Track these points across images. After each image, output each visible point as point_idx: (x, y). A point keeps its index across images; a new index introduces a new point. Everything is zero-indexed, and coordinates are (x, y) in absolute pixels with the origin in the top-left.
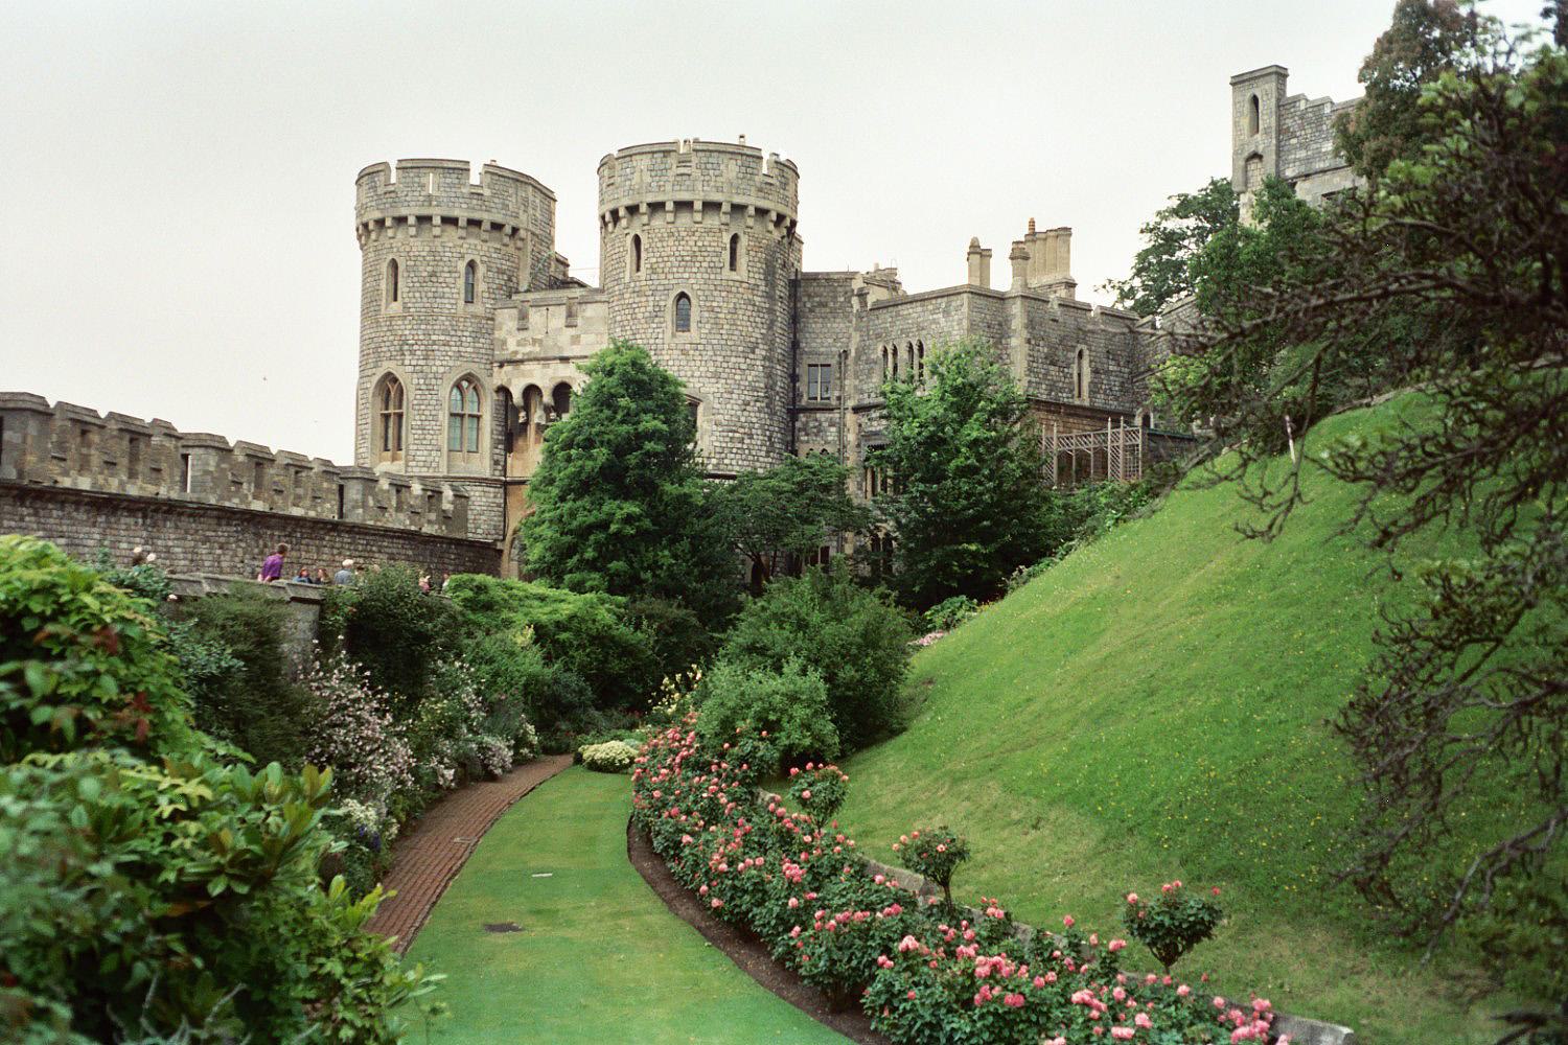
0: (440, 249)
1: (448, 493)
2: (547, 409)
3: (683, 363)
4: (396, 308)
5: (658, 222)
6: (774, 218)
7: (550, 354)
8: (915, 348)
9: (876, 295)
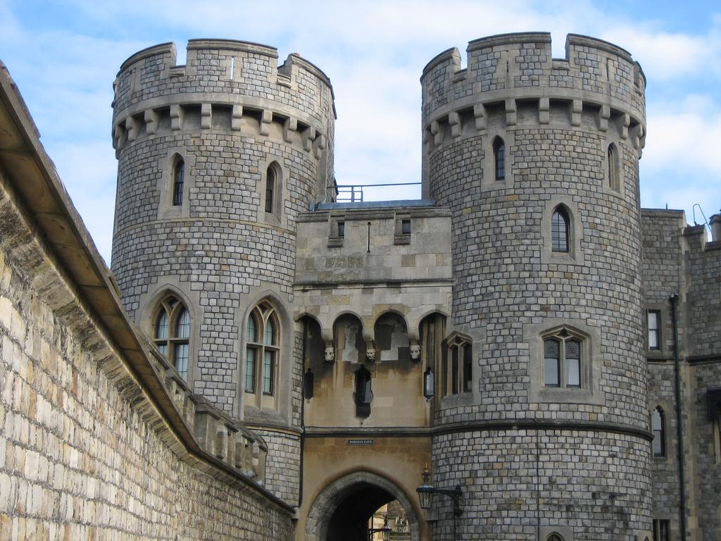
0: (240, 145)
2: (361, 343)
3: (567, 288)
4: (184, 212)
5: (529, 122)
7: (374, 276)
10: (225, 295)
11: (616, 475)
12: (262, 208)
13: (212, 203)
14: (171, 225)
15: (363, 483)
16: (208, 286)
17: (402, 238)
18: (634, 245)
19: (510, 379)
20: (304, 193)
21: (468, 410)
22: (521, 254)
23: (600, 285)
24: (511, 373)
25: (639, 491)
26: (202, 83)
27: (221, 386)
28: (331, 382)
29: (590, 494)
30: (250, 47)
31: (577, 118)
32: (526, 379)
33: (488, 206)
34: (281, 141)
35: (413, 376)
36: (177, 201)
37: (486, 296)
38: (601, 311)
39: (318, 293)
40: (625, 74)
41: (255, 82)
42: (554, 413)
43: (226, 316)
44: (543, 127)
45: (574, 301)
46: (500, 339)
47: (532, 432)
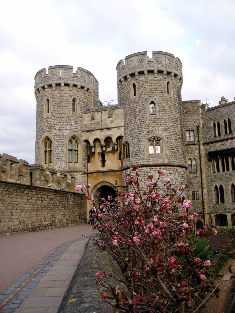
1: (69, 177)
4: (49, 115)
5: (142, 78)
7: (103, 127)
9: (206, 108)
10: (61, 136)
11: (172, 179)
12: (71, 111)
13: (57, 111)
14: (47, 118)
15: (105, 186)
16: (56, 134)
18: (177, 111)
19: (139, 153)
20: (85, 106)
21: (129, 163)
22: (141, 117)
23: (165, 124)
24: (139, 151)
25: (180, 183)
26: (52, 78)
27: (61, 161)
28: (94, 158)
29: (163, 185)
30: (65, 67)
31: (156, 75)
32: (143, 153)
33: (132, 104)
34: (76, 92)
35: (117, 154)
36: (48, 112)
38: (165, 131)
39: (88, 133)
40: (171, 61)
41: (67, 76)
43: (62, 142)
44: (146, 79)
45: (157, 129)
46: (136, 142)
47: (145, 168)
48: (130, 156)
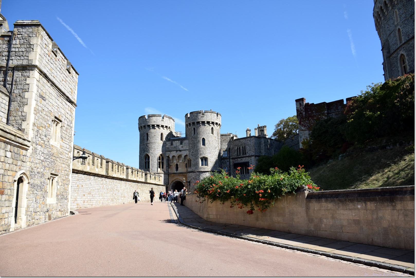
2: (176, 160)
6: (218, 124)
7: (177, 150)
8: (244, 147)
9: (235, 138)
10: (155, 154)
17: (181, 143)
37: (193, 152)
42: (202, 170)
47: (199, 173)
48: (191, 166)
